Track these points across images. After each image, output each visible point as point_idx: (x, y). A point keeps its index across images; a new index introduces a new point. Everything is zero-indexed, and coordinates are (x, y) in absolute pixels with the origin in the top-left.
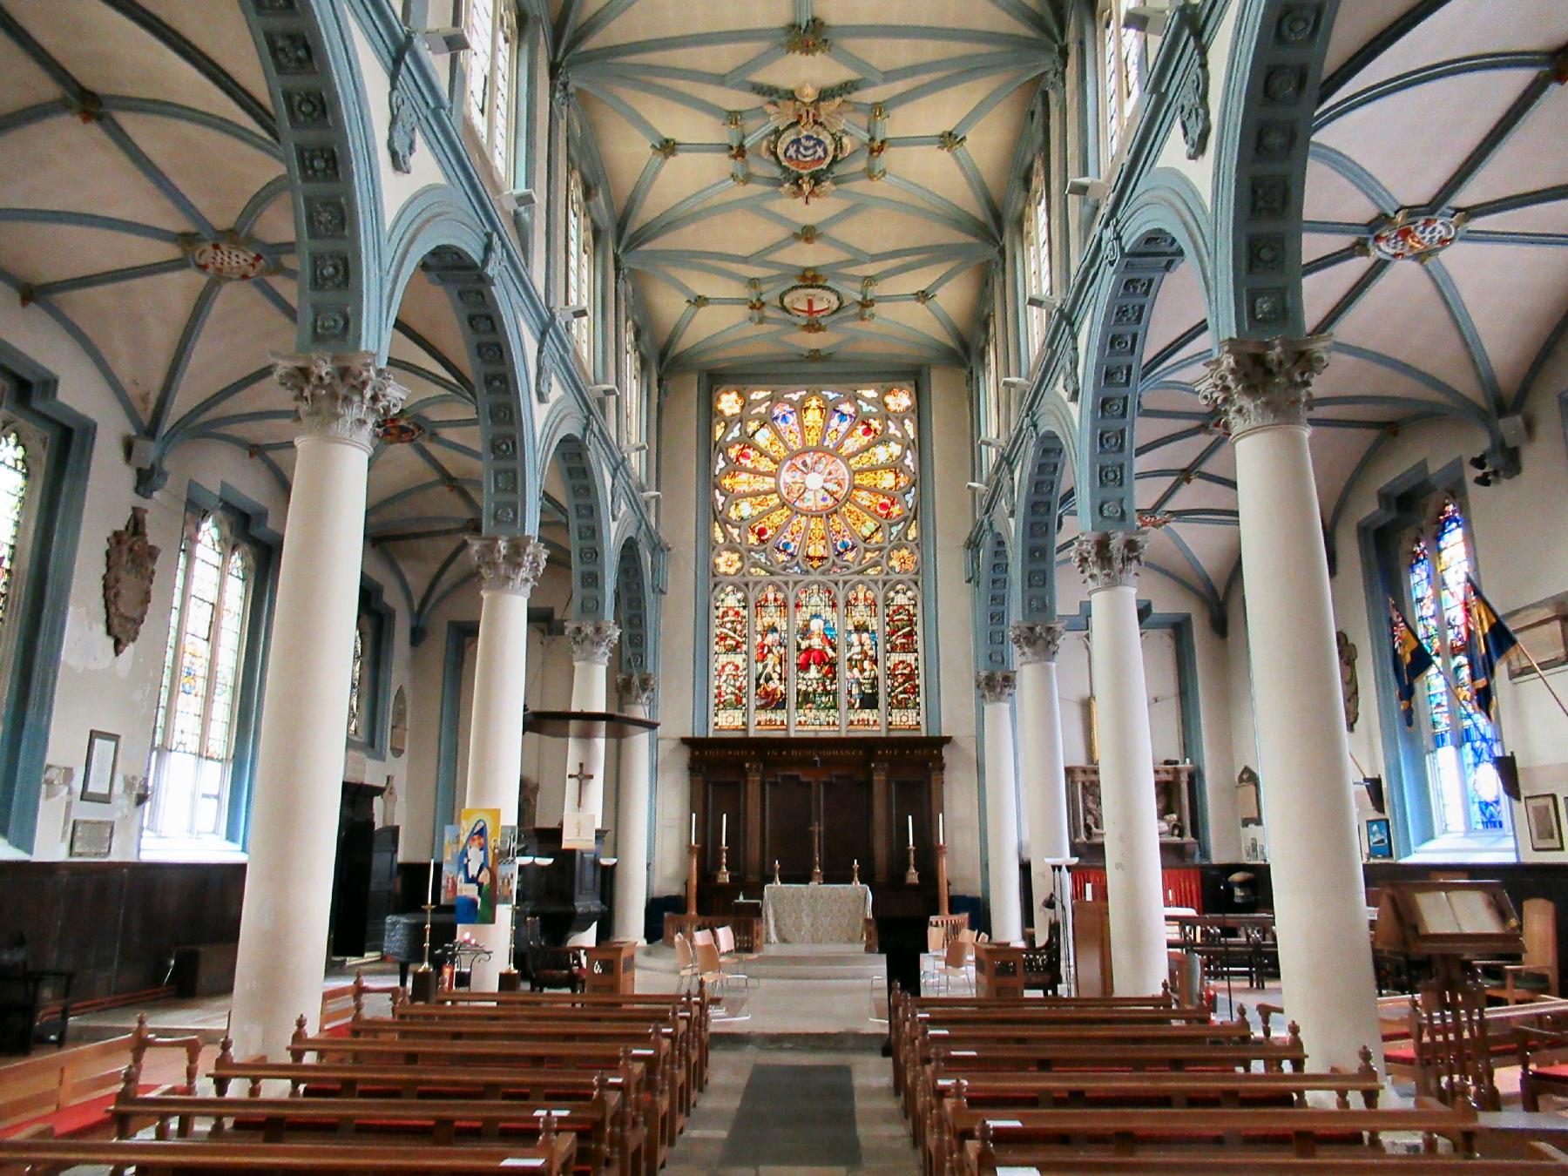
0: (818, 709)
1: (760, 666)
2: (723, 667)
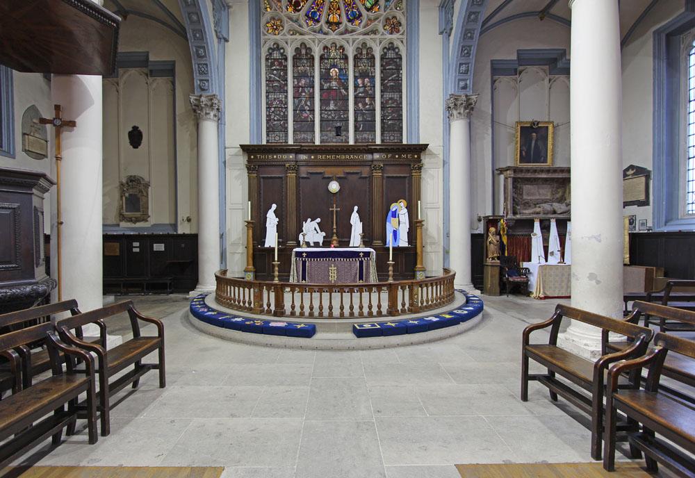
1: (296, 101)
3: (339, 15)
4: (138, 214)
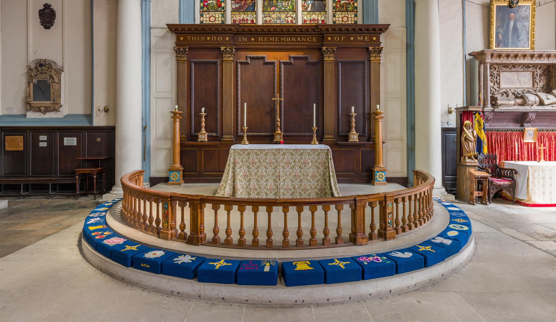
4: (48, 103)
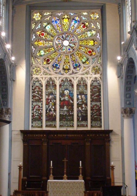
0: (67, 121)
2: (35, 106)
3: (69, 66)
